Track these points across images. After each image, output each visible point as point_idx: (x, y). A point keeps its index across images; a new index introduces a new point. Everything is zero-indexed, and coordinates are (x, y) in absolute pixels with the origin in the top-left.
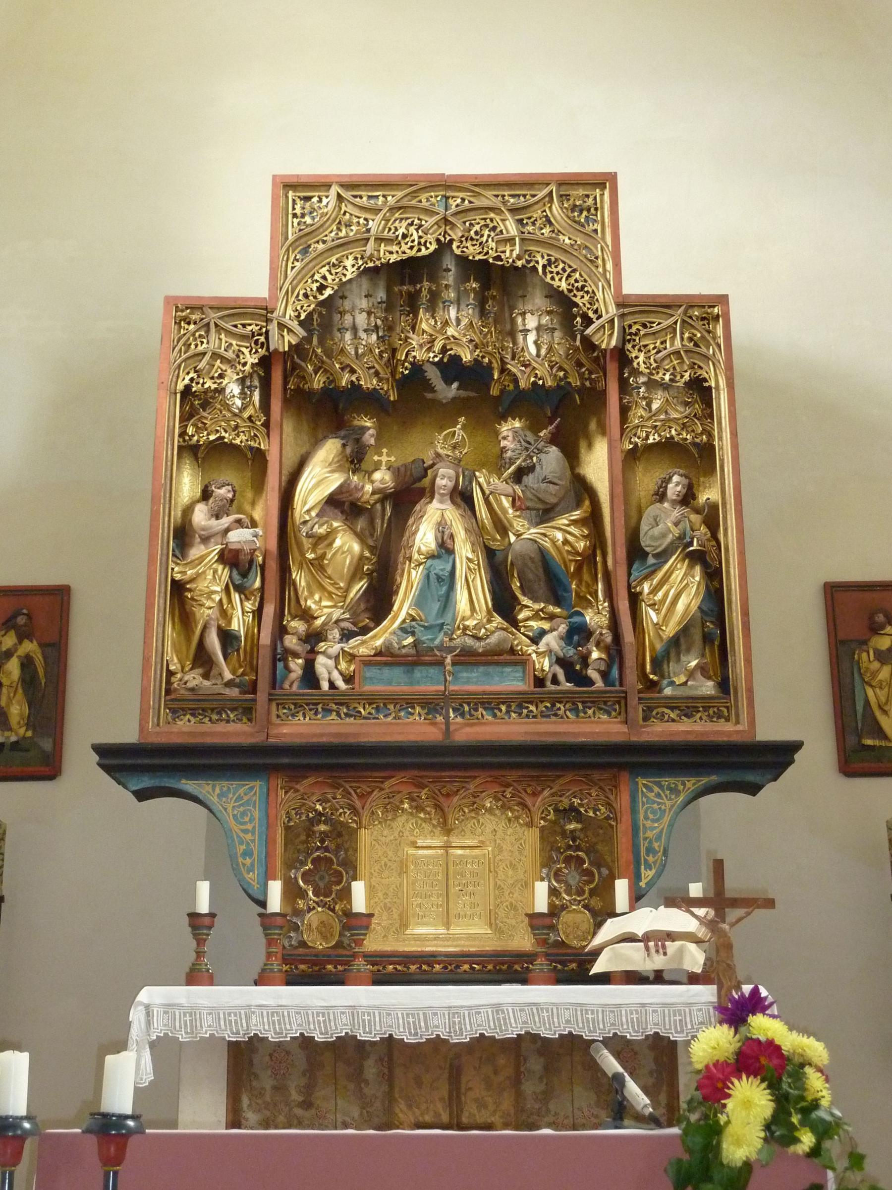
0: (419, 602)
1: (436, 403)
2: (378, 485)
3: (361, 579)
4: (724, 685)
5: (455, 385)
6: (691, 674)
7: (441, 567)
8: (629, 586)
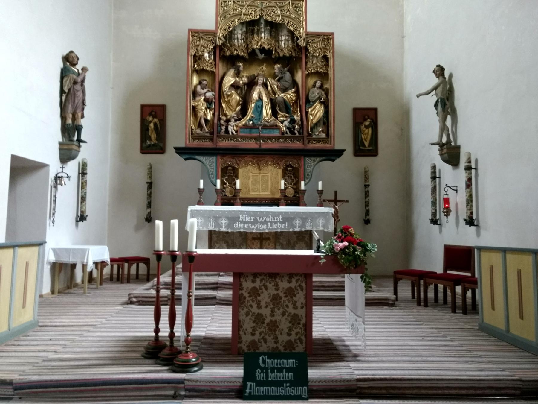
0: (253, 113)
1: (259, 59)
2: (244, 81)
4: (328, 135)
5: (263, 55)
6: (320, 132)
7: (259, 104)
8: (306, 110)
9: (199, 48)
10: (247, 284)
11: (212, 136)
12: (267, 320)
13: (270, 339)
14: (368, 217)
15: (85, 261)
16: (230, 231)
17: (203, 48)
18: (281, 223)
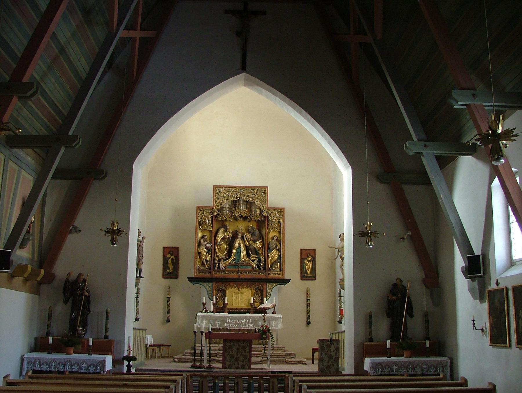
3: (226, 250)
9: (203, 218)
10: (228, 344)
11: (210, 270)
12: (235, 357)
13: (236, 363)
14: (309, 320)
15: (146, 342)
16: (221, 328)
17: (205, 217)
18: (251, 323)
